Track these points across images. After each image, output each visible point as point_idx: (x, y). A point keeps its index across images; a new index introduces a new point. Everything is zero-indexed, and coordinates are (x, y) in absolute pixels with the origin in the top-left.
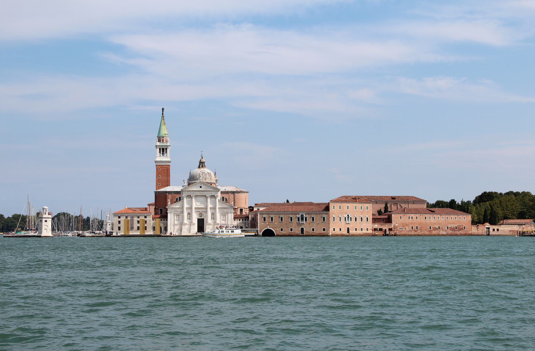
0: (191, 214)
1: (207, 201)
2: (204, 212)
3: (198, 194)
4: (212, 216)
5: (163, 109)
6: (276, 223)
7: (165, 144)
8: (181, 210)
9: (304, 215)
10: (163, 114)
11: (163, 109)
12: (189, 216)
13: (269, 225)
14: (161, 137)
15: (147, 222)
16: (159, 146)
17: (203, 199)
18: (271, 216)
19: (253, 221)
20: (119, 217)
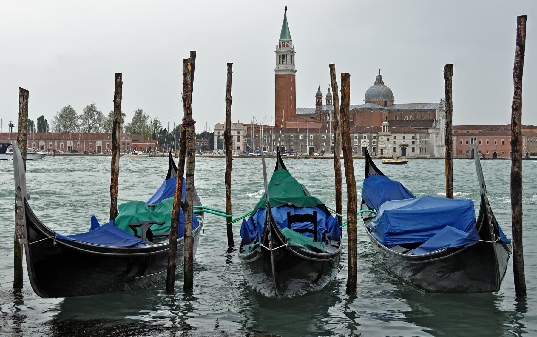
5: (286, 8)
10: (285, 13)
11: (286, 8)
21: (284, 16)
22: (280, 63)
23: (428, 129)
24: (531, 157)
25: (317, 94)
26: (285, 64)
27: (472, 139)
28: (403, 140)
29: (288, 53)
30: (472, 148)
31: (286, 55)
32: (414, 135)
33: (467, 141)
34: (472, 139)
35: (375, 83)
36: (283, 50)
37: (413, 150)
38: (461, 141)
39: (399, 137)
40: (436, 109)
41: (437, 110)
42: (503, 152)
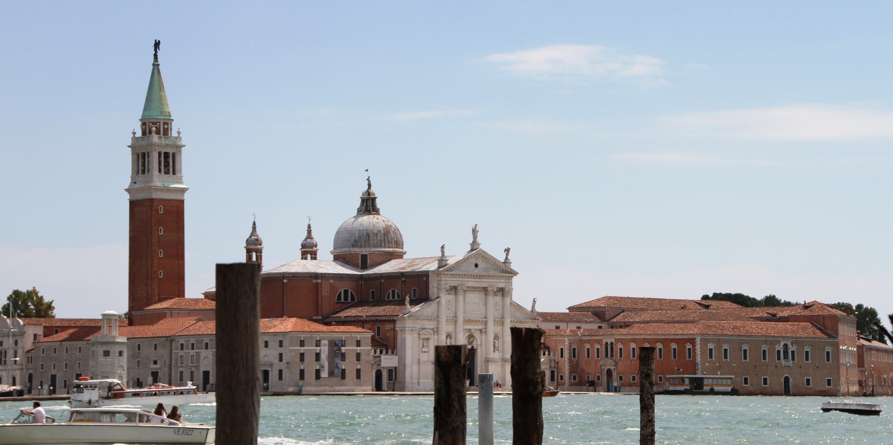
0: (453, 335)
1: (486, 304)
2: (478, 332)
3: (471, 283)
4: (494, 342)
5: (157, 45)
6: (734, 365)
7: (169, 142)
8: (430, 325)
10: (156, 56)
11: (157, 45)
12: (449, 340)
13: (719, 368)
14: (162, 122)
15: (362, 357)
16: (159, 146)
17: (474, 298)
18: (725, 346)
19: (574, 356)
20: (302, 344)
22: (138, 173)
23: (394, 321)
24: (671, 388)
26: (146, 173)
27: (607, 343)
29: (150, 148)
30: (606, 368)
34: (607, 343)
35: (359, 211)
36: (143, 143)
38: (588, 349)
40: (428, 271)
41: (430, 273)
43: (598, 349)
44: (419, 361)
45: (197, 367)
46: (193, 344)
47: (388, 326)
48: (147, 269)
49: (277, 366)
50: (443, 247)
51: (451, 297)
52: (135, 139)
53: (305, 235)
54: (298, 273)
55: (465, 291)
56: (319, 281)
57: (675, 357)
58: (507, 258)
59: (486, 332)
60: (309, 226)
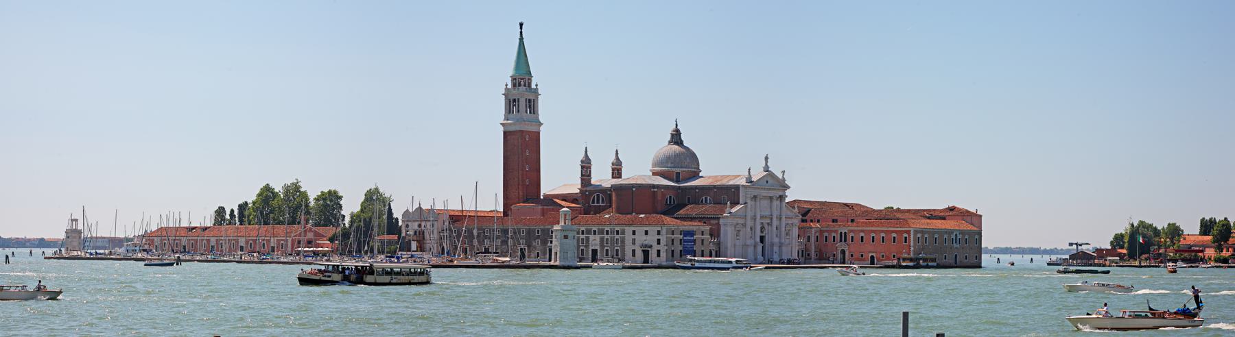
1: (771, 208)
3: (765, 193)
5: (521, 25)
9: (958, 235)
10: (521, 32)
11: (521, 25)
14: (527, 77)
15: (705, 242)
17: (765, 203)
18: (926, 236)
21: (519, 36)
22: (510, 112)
23: (718, 218)
25: (582, 162)
27: (841, 233)
28: (645, 237)
31: (518, 99)
32: (659, 229)
33: (834, 237)
34: (841, 233)
35: (670, 143)
37: (659, 255)
38: (826, 237)
39: (640, 230)
42: (883, 256)
43: (834, 237)
44: (735, 245)
45: (587, 247)
46: (583, 231)
47: (713, 222)
48: (519, 179)
49: (656, 247)
50: (749, 169)
51: (753, 203)
52: (507, 89)
53: (614, 156)
54: (643, 184)
55: (760, 199)
56: (656, 190)
57: (894, 242)
58: (783, 177)
59: (771, 225)
60: (617, 151)
